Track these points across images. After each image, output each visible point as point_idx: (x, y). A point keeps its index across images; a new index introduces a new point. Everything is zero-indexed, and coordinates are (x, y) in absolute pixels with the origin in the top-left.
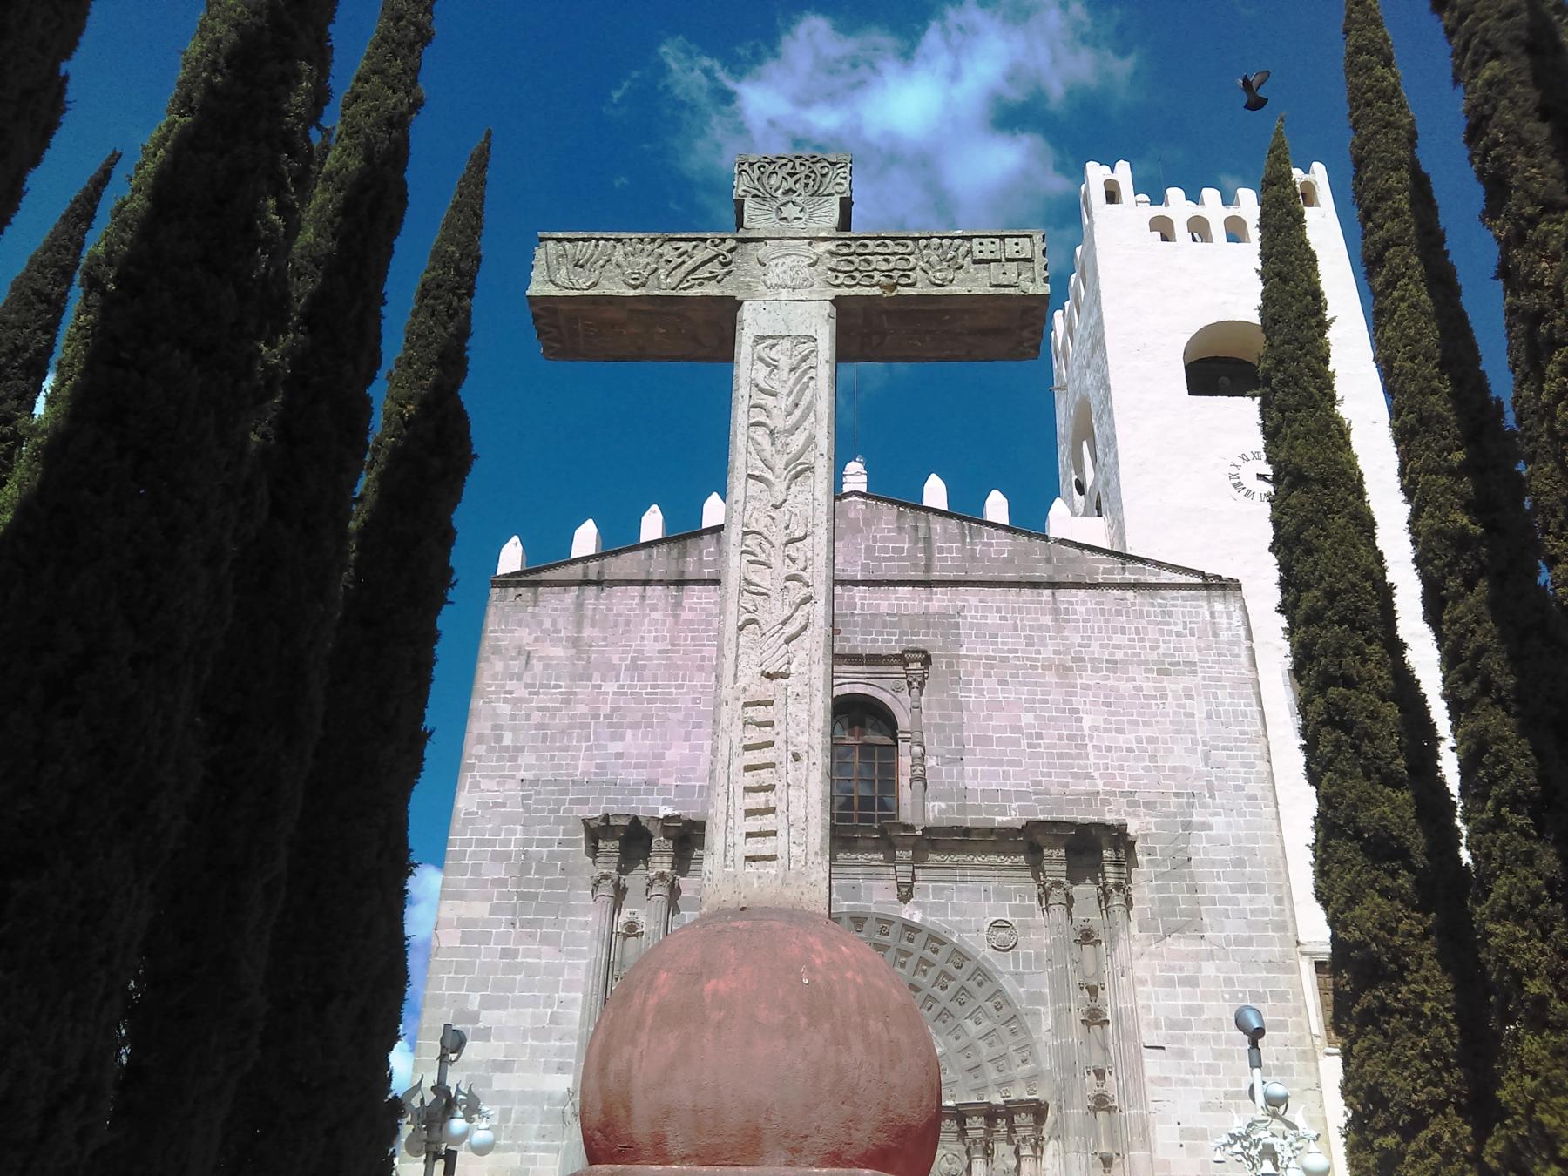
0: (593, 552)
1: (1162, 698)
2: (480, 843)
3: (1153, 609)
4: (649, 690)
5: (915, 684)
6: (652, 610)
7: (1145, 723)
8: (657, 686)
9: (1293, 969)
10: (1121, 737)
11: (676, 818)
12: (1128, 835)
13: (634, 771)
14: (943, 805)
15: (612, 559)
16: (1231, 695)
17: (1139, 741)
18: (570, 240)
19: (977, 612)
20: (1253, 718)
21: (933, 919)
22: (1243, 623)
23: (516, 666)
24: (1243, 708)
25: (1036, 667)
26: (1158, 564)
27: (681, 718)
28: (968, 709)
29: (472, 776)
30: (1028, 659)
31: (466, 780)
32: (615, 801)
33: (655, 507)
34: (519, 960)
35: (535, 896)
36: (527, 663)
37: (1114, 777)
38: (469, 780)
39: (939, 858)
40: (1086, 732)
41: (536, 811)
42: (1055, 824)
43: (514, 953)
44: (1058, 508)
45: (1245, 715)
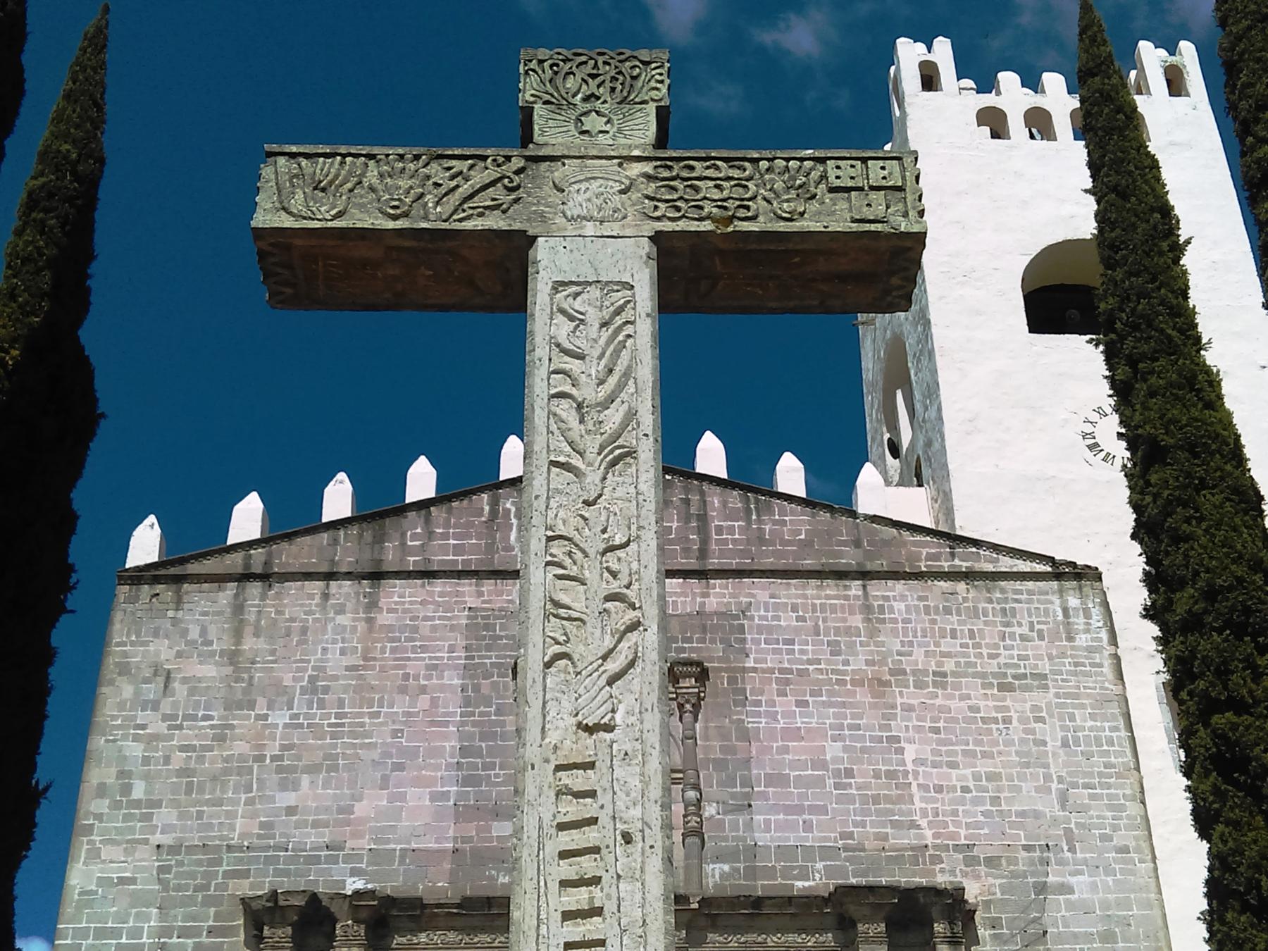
0: (257, 535)
1: (1004, 722)
3: (990, 606)
4: (333, 721)
5: (688, 707)
6: (338, 613)
7: (985, 755)
8: (345, 715)
10: (954, 772)
11: (371, 894)
12: (966, 902)
15: (285, 545)
16: (1093, 717)
17: (977, 777)
18: (307, 156)
19: (767, 610)
20: (1120, 745)
22: (1105, 624)
23: (151, 690)
24: (1107, 733)
25: (841, 682)
26: (996, 548)
27: (376, 758)
28: (759, 740)
29: (89, 842)
30: (834, 671)
31: (82, 847)
32: (286, 873)
33: (342, 476)
36: (166, 687)
37: (945, 824)
38: (86, 847)
39: (721, 939)
40: (910, 767)
41: (178, 888)
42: (871, 889)
44: (868, 476)
45: (1111, 742)
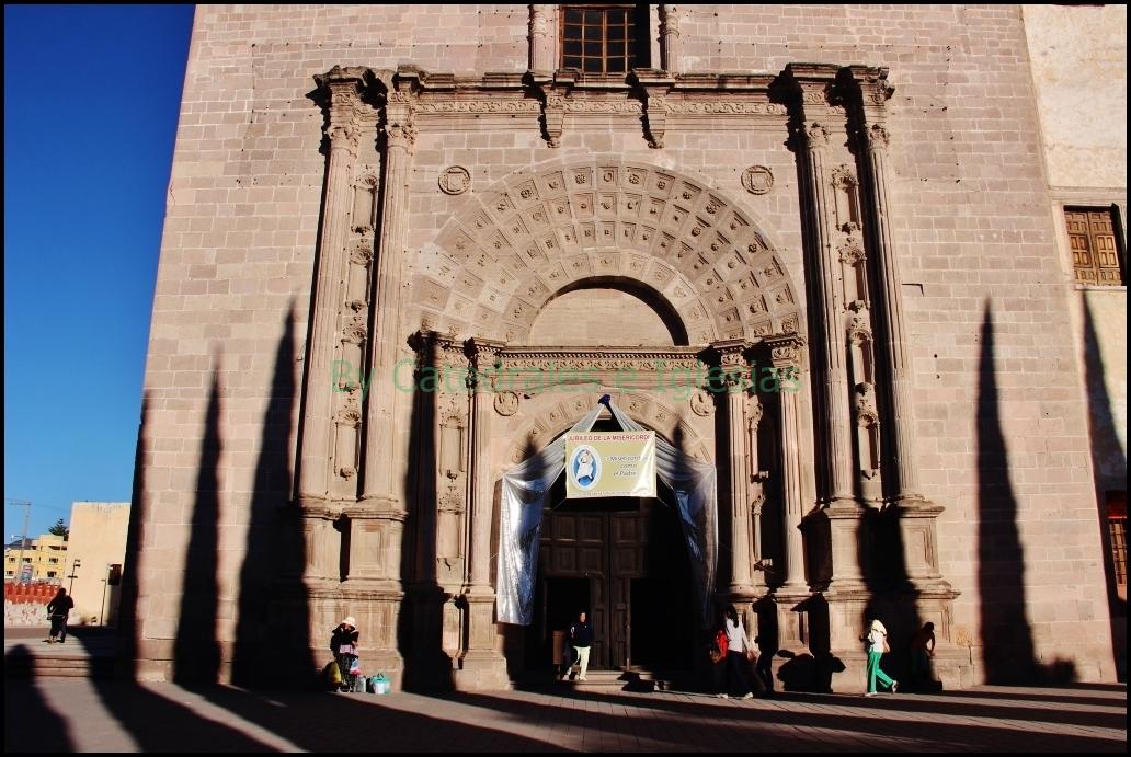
2: (213, 107)
9: (1046, 212)
13: (371, 33)
14: (697, 59)
21: (688, 166)
34: (254, 216)
35: (270, 155)
37: (870, 31)
43: (250, 210)
